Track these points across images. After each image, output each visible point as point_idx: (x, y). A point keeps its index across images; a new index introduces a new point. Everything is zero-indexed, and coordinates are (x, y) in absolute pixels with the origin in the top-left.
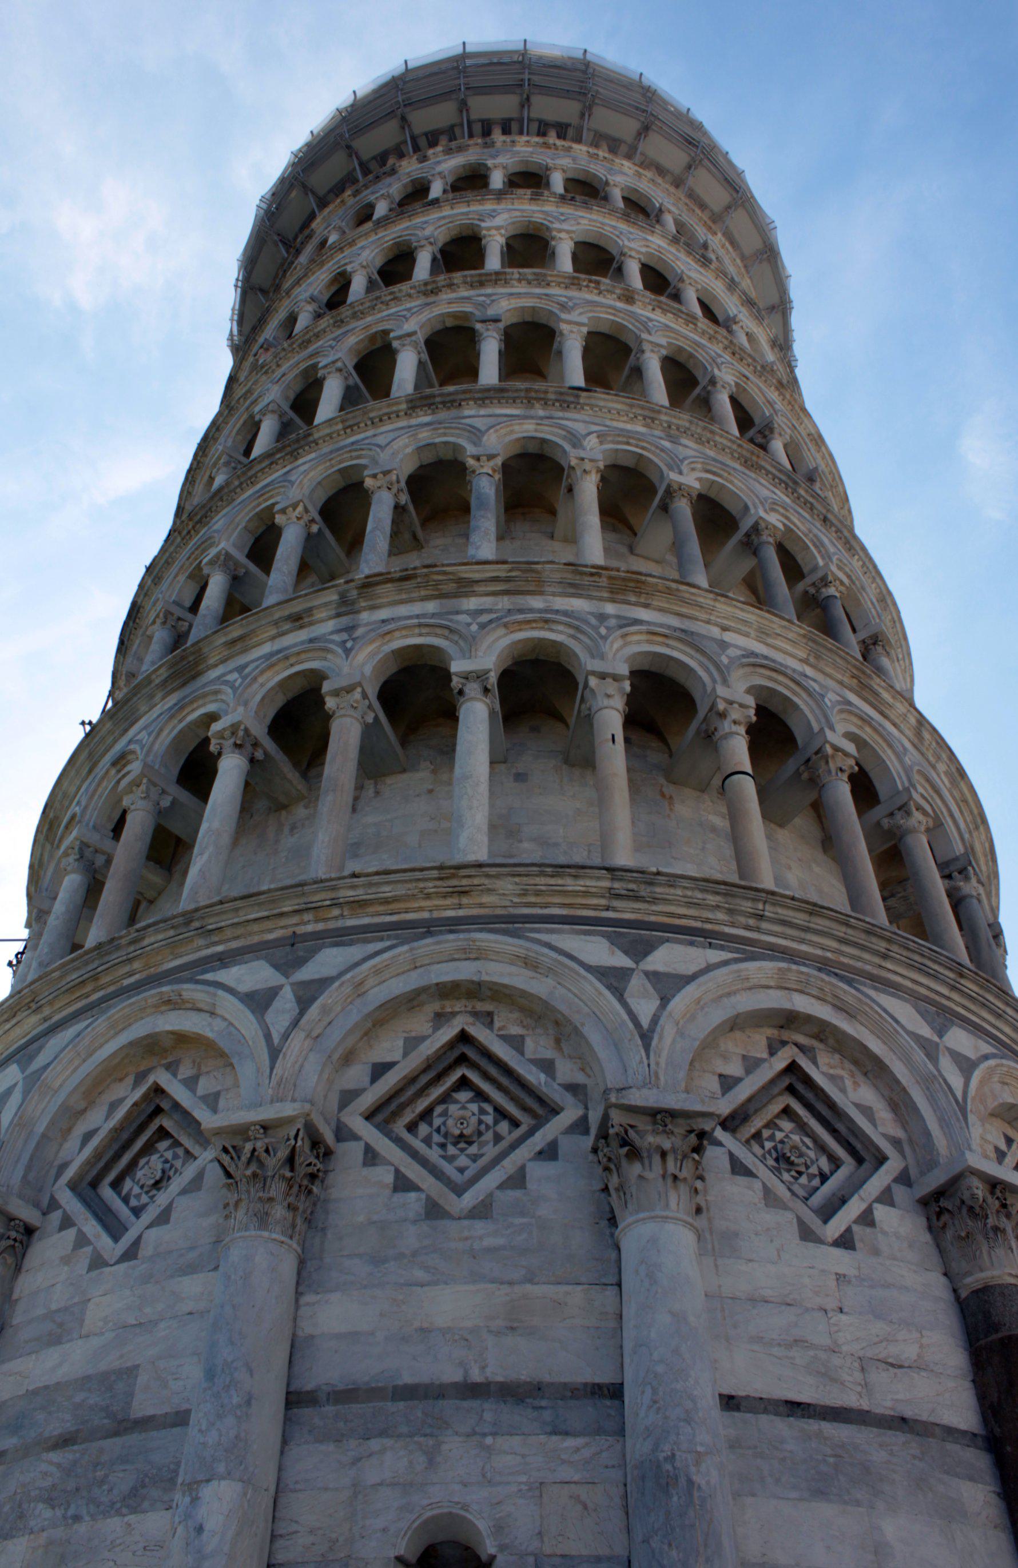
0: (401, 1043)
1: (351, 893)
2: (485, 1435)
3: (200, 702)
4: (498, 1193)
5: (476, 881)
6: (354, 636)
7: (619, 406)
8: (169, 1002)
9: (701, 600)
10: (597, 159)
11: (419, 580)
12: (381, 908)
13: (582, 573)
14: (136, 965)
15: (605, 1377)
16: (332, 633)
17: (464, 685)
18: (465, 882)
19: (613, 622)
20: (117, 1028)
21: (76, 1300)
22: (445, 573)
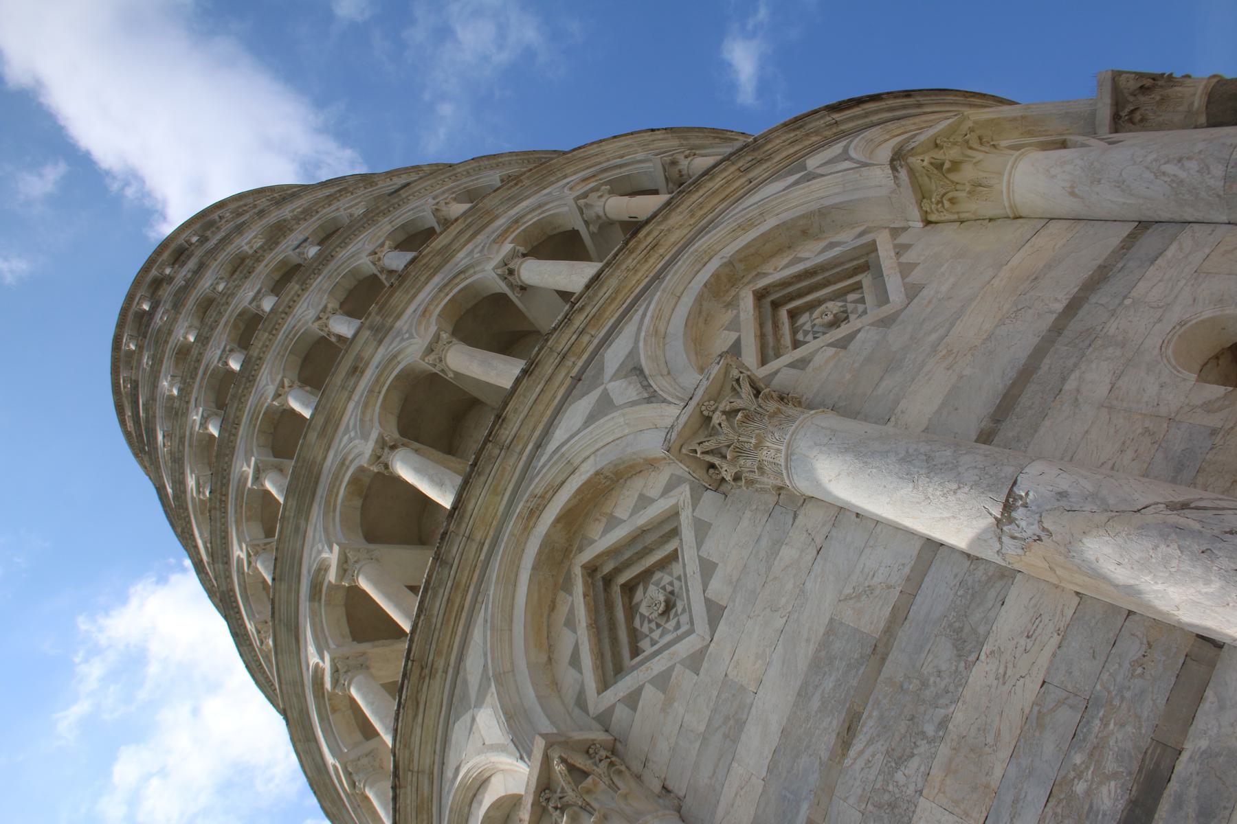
4: (907, 280)
5: (655, 233)
8: (532, 512)
12: (613, 306)
18: (649, 239)
20: (511, 582)
21: (715, 693)
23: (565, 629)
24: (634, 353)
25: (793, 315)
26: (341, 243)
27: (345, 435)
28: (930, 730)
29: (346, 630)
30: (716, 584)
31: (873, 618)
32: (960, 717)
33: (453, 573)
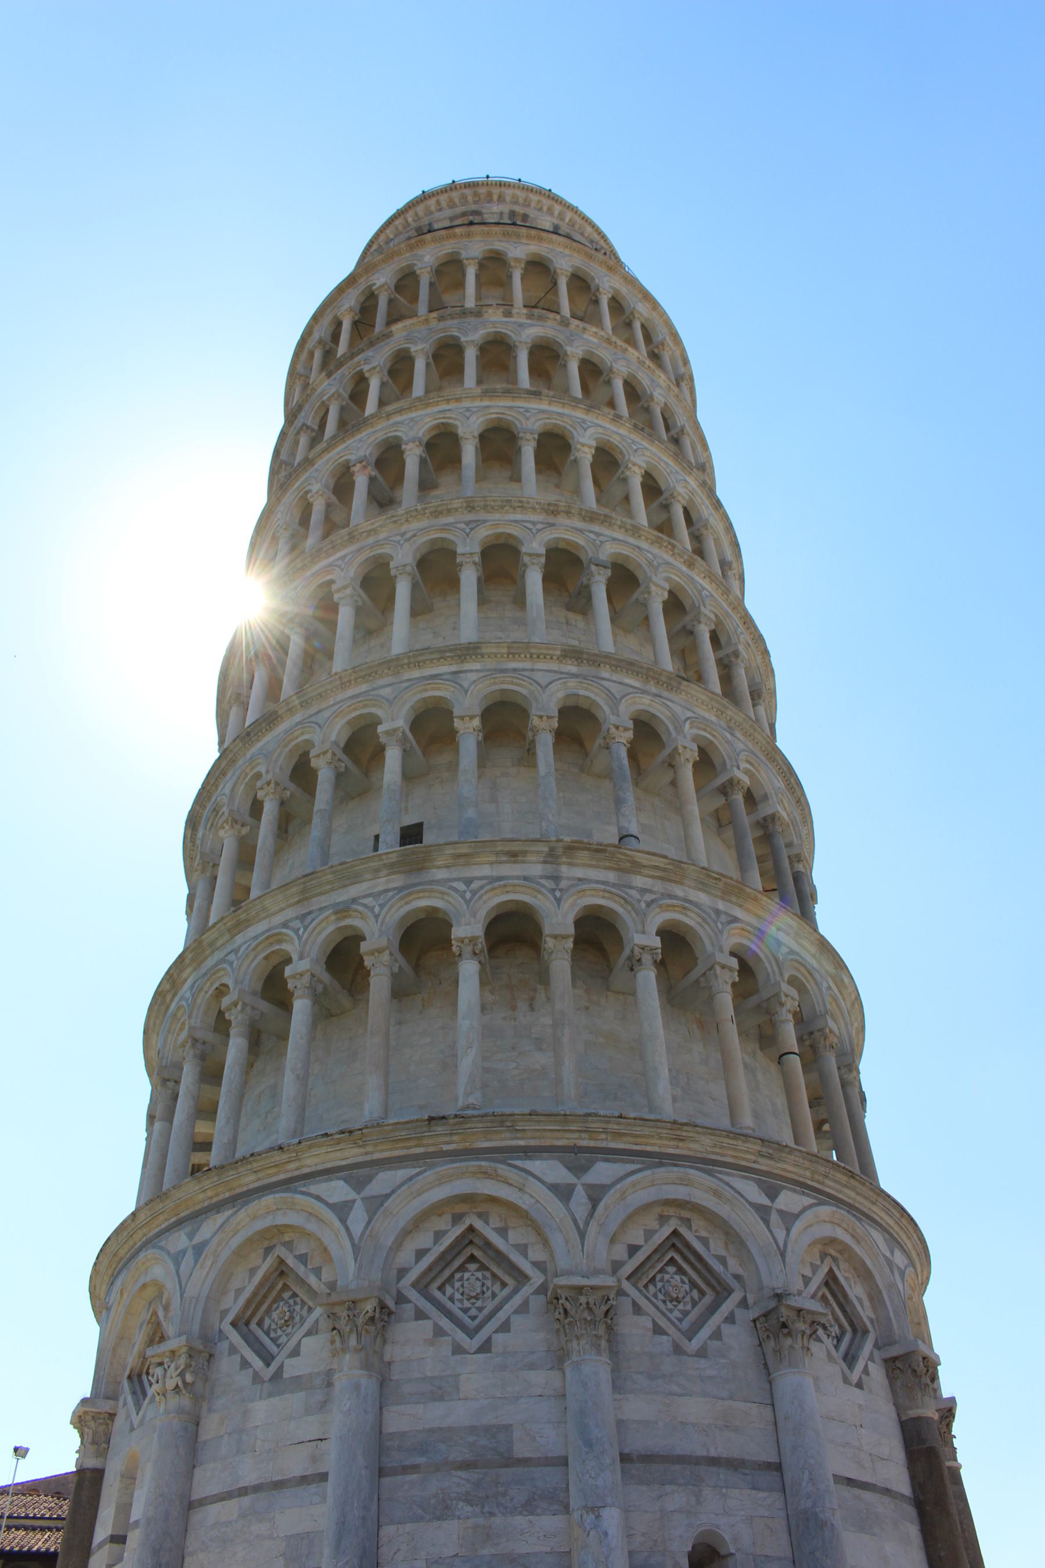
0: (642, 1233)
1: (616, 1127)
2: (722, 1487)
3: (426, 894)
4: (709, 1342)
5: (691, 1134)
6: (560, 887)
7: (704, 697)
8: (485, 1173)
9: (772, 908)
10: (643, 366)
11: (607, 855)
12: (632, 1140)
13: (710, 876)
14: (455, 1138)
15: (773, 1458)
16: (541, 877)
17: (641, 954)
18: (684, 1134)
19: (723, 918)
20: (441, 1181)
22: (625, 854)
23: (432, 1234)
24: (604, 1189)
25: (672, 1261)
26: (614, 665)
27: (464, 883)
28: (486, 1509)
29: (328, 952)
30: (499, 1339)
31: (521, 1450)
32: (498, 1520)
33: (426, 1134)
